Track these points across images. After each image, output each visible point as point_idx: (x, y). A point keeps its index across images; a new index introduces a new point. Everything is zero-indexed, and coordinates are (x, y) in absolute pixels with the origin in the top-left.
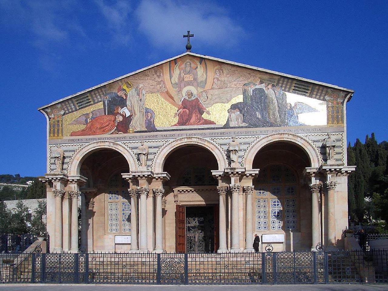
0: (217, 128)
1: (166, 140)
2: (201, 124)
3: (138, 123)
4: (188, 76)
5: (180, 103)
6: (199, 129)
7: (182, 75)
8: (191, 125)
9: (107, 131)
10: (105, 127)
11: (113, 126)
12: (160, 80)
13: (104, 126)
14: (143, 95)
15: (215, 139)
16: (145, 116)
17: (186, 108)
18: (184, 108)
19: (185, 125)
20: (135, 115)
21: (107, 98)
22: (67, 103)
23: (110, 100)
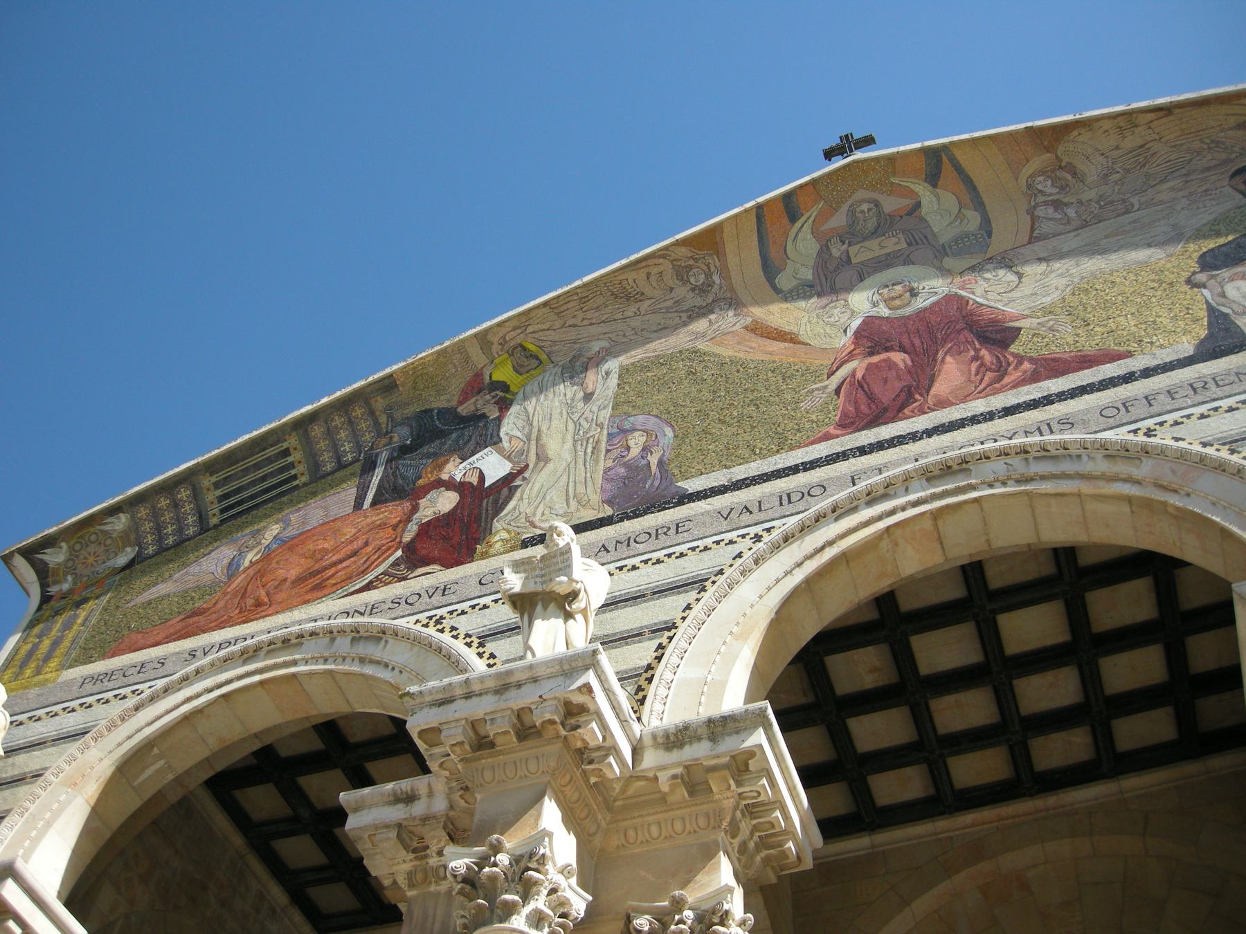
0: (1147, 373)
1: (757, 529)
2: (1014, 387)
3: (556, 498)
4: (873, 244)
5: (844, 341)
6: (1008, 411)
7: (837, 251)
8: (942, 404)
9: (335, 584)
10: (341, 561)
11: (389, 549)
12: (710, 298)
13: (335, 558)
14: (608, 373)
15: (1161, 424)
16: (608, 451)
17: (887, 349)
18: (871, 354)
19: (893, 419)
20: (542, 464)
21: (396, 439)
22: (163, 502)
23: (408, 442)
